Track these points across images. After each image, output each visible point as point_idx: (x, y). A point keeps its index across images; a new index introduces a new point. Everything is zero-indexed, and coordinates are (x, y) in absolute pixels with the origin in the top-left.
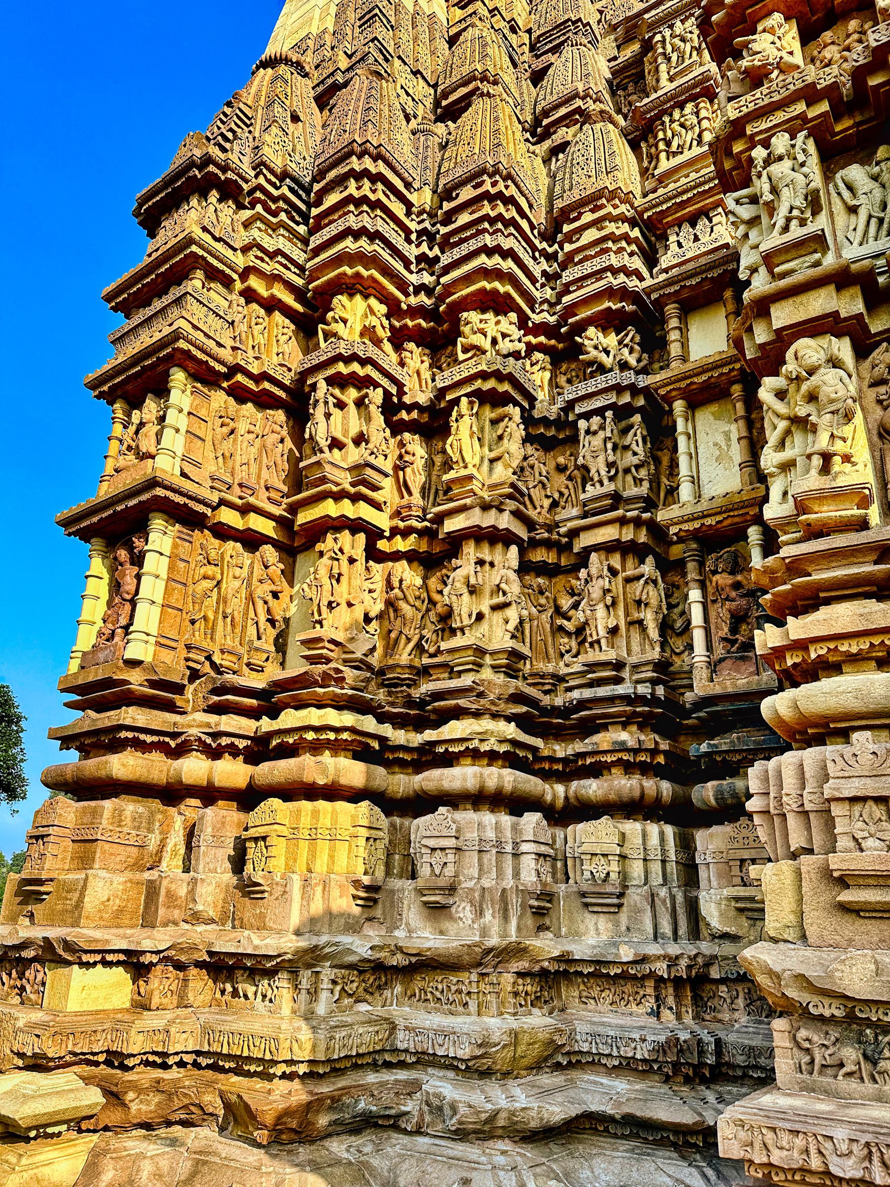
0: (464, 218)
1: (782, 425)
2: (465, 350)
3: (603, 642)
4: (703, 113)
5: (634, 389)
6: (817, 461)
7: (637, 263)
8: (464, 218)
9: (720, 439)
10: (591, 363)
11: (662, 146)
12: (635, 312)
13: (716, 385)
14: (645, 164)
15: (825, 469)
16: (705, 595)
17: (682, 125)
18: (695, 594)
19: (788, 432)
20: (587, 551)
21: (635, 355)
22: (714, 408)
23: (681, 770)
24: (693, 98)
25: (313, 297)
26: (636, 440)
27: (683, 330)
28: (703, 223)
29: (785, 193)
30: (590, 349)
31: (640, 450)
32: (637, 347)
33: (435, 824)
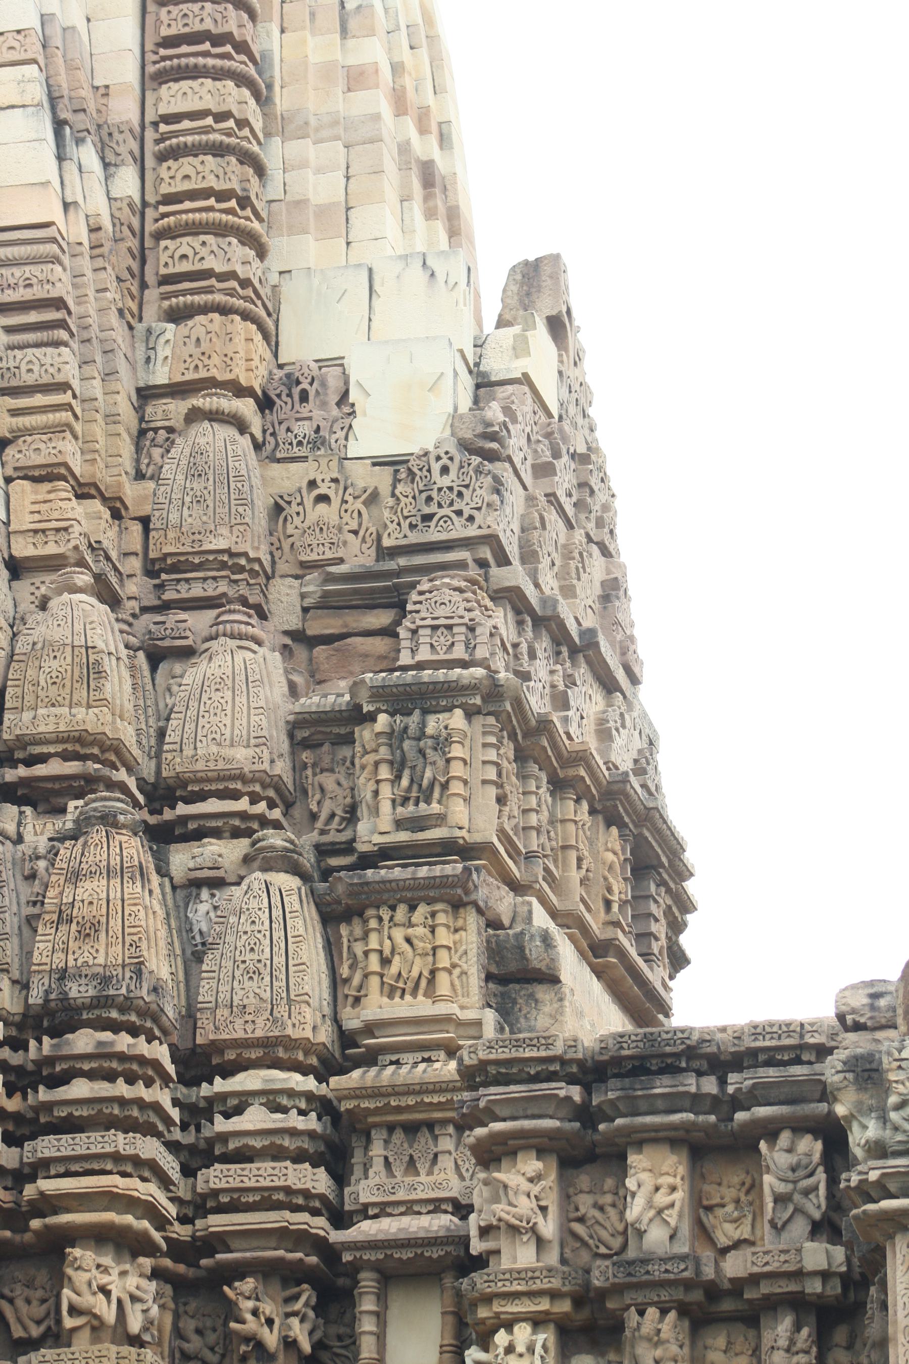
2: (74, 1310)
4: (443, 937)
8: (80, 1089)
10: (248, 1339)
12: (317, 1266)
21: (308, 1326)
27: (381, 1317)
28: (424, 1137)
30: (249, 1317)
32: (311, 1314)
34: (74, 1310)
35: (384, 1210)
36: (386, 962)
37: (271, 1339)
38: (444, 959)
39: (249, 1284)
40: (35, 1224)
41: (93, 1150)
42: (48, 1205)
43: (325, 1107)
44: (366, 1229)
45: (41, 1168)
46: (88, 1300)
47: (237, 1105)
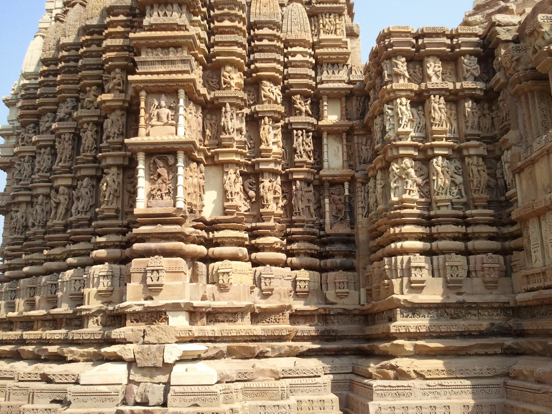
0: (265, 42)
1: (397, 177)
2: (265, 96)
3: (302, 213)
4: (337, 21)
5: (312, 124)
6: (408, 191)
7: (313, 73)
9: (336, 148)
11: (321, 26)
13: (339, 131)
14: (313, 29)
15: (409, 194)
16: (330, 200)
17: (330, 21)
18: (327, 200)
19: (397, 179)
20: (295, 180)
22: (334, 137)
23: (320, 256)
24: (335, 13)
25: (215, 61)
26: (309, 140)
29: (404, 117)
31: (311, 145)
33: (266, 270)
34: (265, 96)
35: (328, 82)
36: (324, 26)
37: (304, 109)
38: (338, 26)
39: (299, 96)
40: (254, 75)
41: (269, 57)
42: (257, 70)
43: (315, 56)
44: (325, 86)
45: (256, 61)
46: (268, 94)
47: (294, 54)
